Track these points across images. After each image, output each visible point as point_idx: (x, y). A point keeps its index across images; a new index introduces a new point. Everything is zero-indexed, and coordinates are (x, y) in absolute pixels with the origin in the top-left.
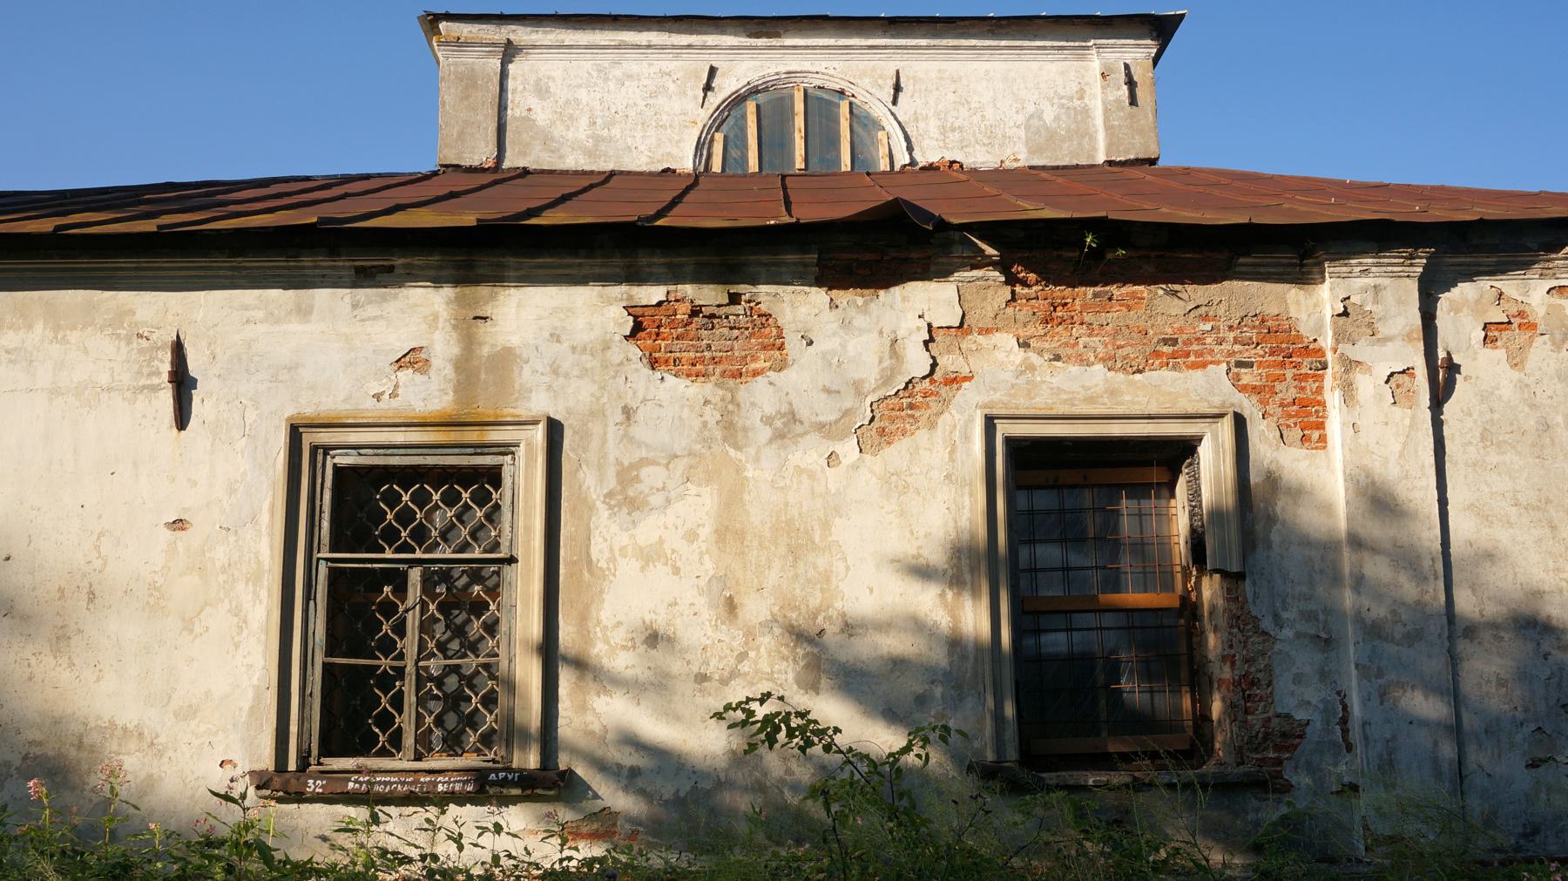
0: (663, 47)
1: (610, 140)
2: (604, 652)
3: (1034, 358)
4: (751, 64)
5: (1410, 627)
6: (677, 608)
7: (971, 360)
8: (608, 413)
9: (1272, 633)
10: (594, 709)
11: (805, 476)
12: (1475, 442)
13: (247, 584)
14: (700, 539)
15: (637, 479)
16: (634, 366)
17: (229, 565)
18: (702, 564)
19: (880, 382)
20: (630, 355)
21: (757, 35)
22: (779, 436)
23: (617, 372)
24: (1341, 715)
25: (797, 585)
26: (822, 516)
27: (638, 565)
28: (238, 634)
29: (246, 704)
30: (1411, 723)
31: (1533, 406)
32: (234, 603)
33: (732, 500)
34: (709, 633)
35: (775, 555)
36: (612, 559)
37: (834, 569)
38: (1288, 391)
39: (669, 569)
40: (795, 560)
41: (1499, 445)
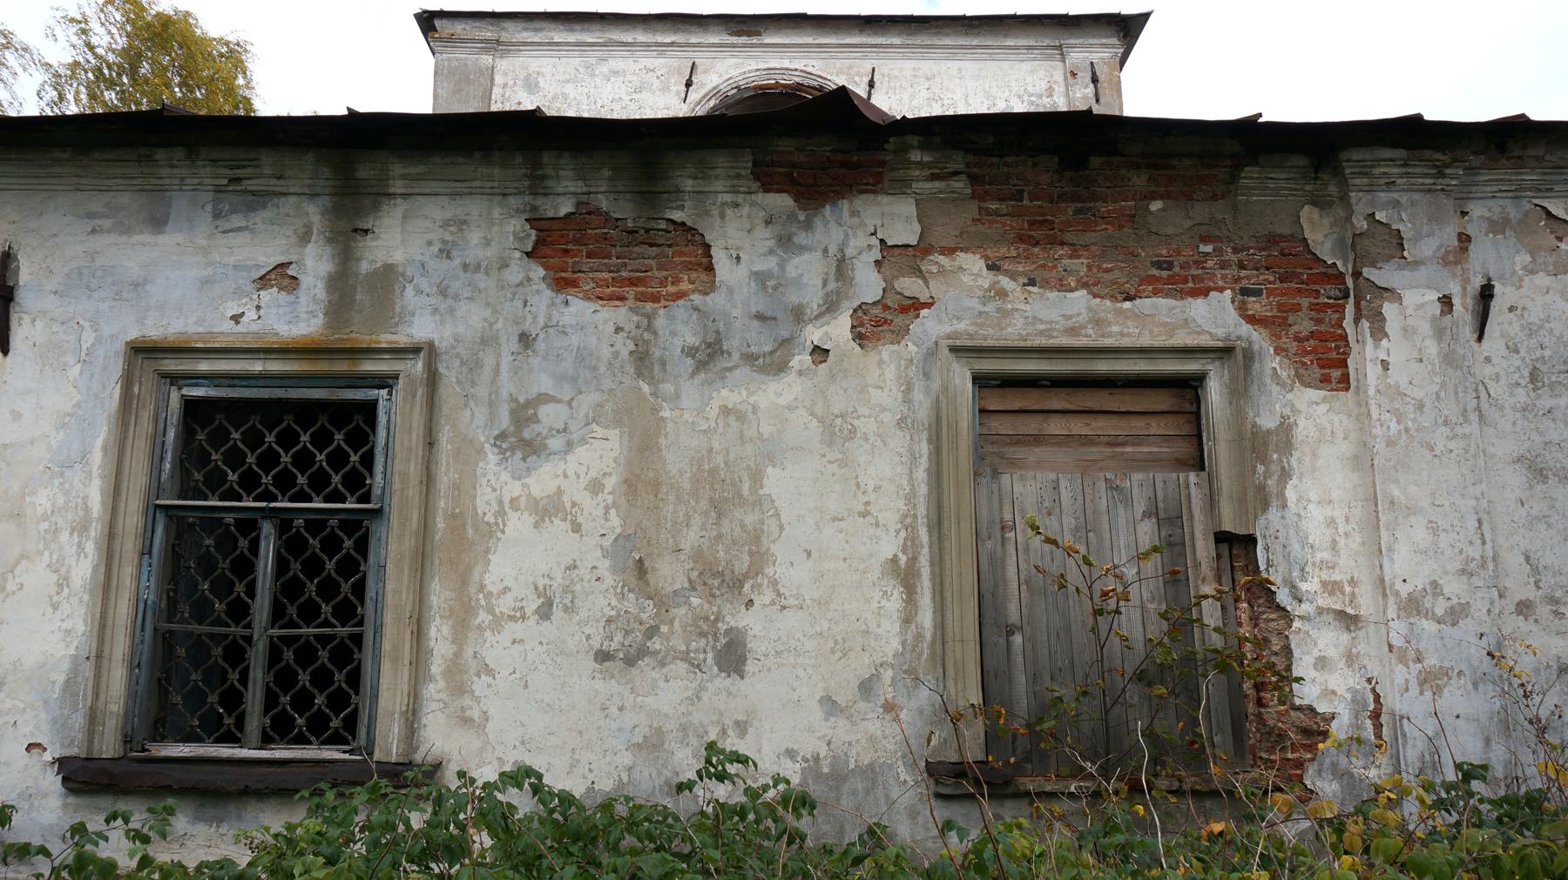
0: (647, 45)
2: (487, 623)
3: (1005, 282)
4: (732, 61)
5: (1455, 601)
6: (576, 571)
7: (932, 284)
8: (503, 340)
9: (1289, 608)
10: (472, 692)
11: (732, 419)
12: (1523, 383)
13: (71, 534)
14: (606, 491)
15: (535, 419)
16: (535, 287)
17: (53, 511)
18: (607, 520)
19: (824, 308)
20: (532, 275)
21: (739, 34)
22: (701, 366)
23: (514, 294)
24: (1371, 707)
25: (720, 547)
26: (752, 465)
27: (532, 520)
28: (58, 593)
29: (61, 678)
30: (1458, 717)
32: (55, 557)
33: (644, 446)
34: (614, 603)
35: (695, 511)
36: (501, 513)
37: (765, 528)
38: (1303, 324)
39: (568, 525)
40: (719, 517)
41: (1552, 386)
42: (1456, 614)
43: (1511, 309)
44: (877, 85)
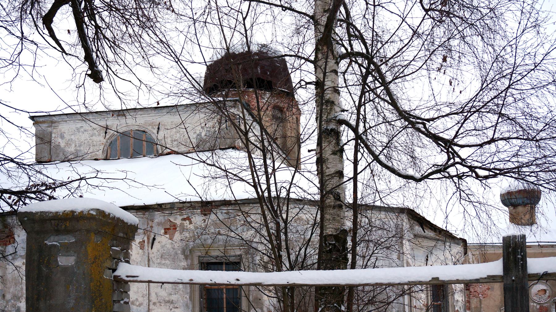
1: (80, 151)
31: (174, 249)
41: (165, 258)
42: (140, 305)
43: (159, 242)
44: (160, 128)
